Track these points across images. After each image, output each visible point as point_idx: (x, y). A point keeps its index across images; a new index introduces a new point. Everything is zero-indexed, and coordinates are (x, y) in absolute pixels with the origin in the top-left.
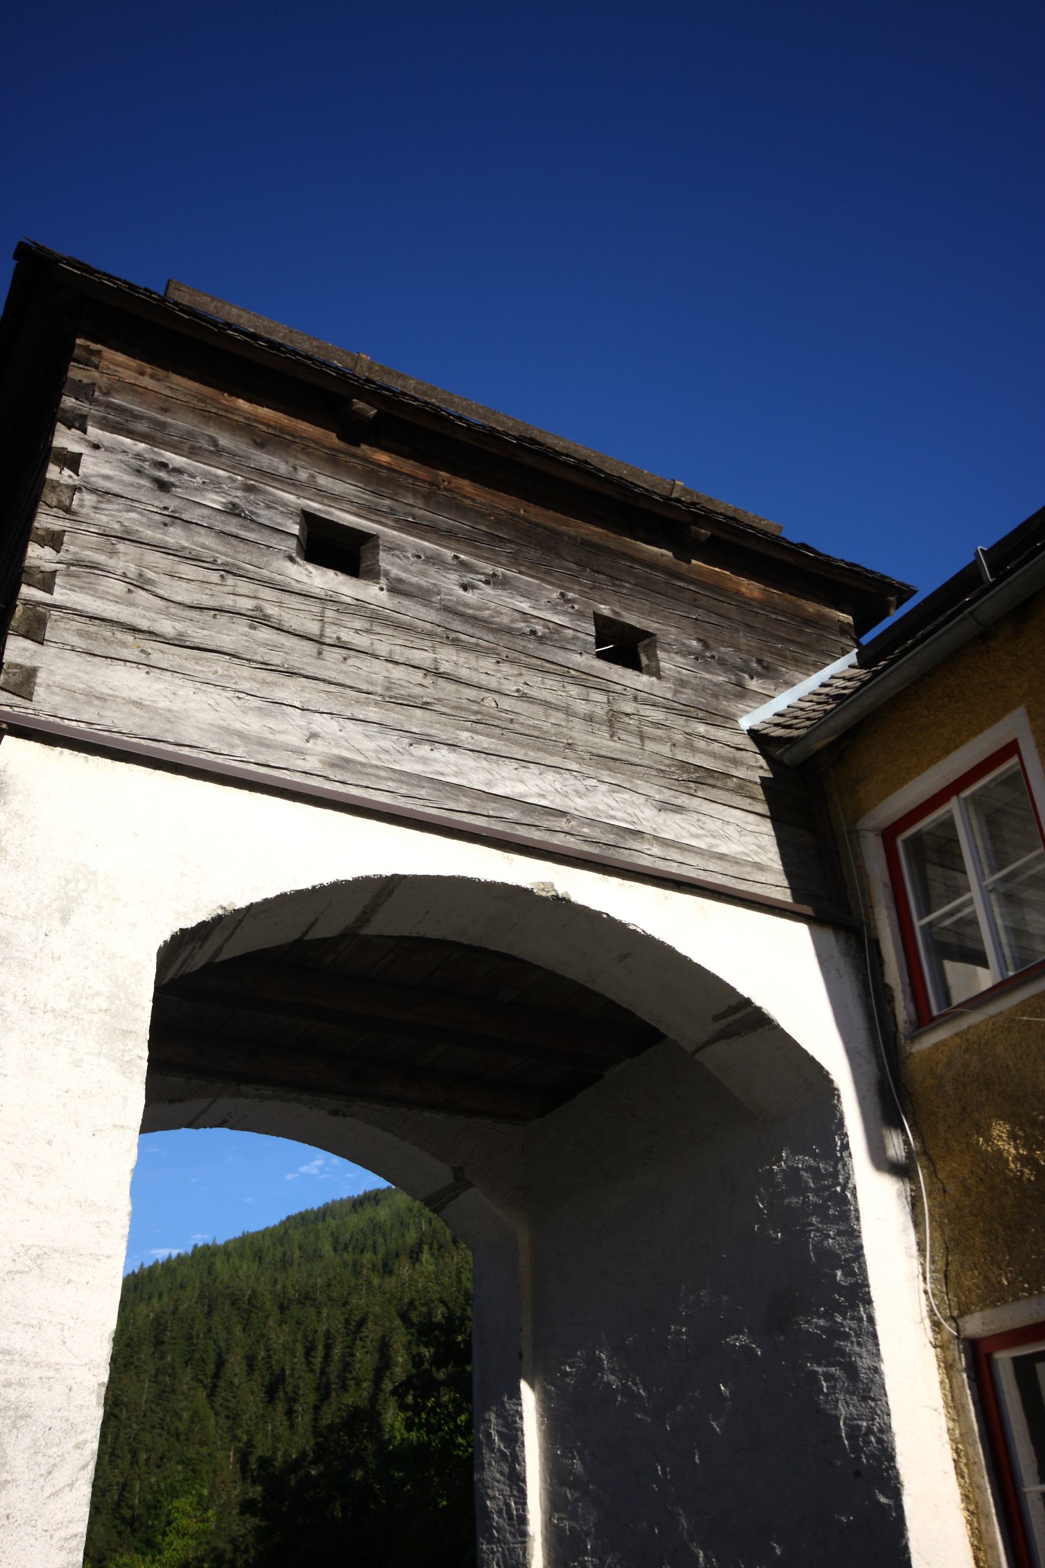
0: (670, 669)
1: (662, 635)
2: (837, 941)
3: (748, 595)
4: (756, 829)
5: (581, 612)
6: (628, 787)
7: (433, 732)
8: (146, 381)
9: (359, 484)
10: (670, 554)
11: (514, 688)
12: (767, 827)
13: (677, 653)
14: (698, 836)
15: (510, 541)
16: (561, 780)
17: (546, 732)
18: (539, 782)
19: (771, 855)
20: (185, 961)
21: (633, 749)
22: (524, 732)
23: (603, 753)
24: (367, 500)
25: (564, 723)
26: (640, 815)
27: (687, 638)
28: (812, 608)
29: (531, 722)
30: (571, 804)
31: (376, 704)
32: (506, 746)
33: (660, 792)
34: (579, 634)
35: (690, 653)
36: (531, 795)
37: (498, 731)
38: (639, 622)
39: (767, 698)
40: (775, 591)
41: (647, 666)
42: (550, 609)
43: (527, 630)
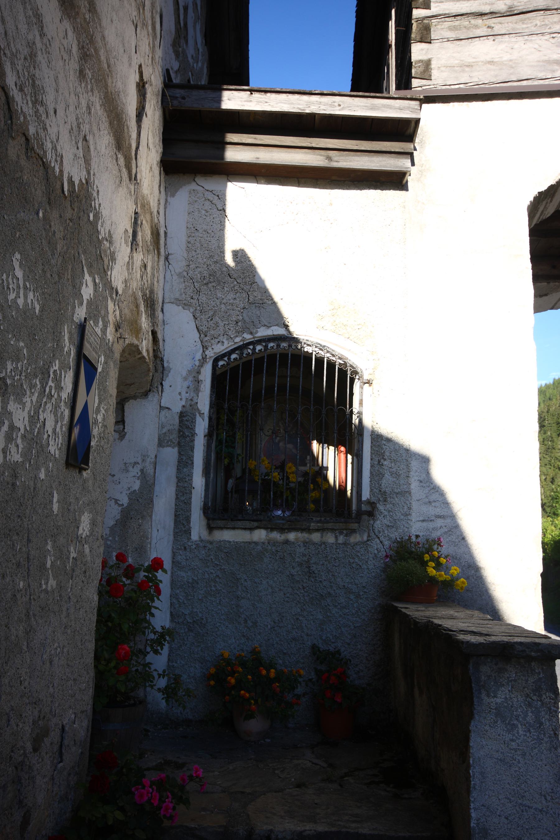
20: (542, 212)
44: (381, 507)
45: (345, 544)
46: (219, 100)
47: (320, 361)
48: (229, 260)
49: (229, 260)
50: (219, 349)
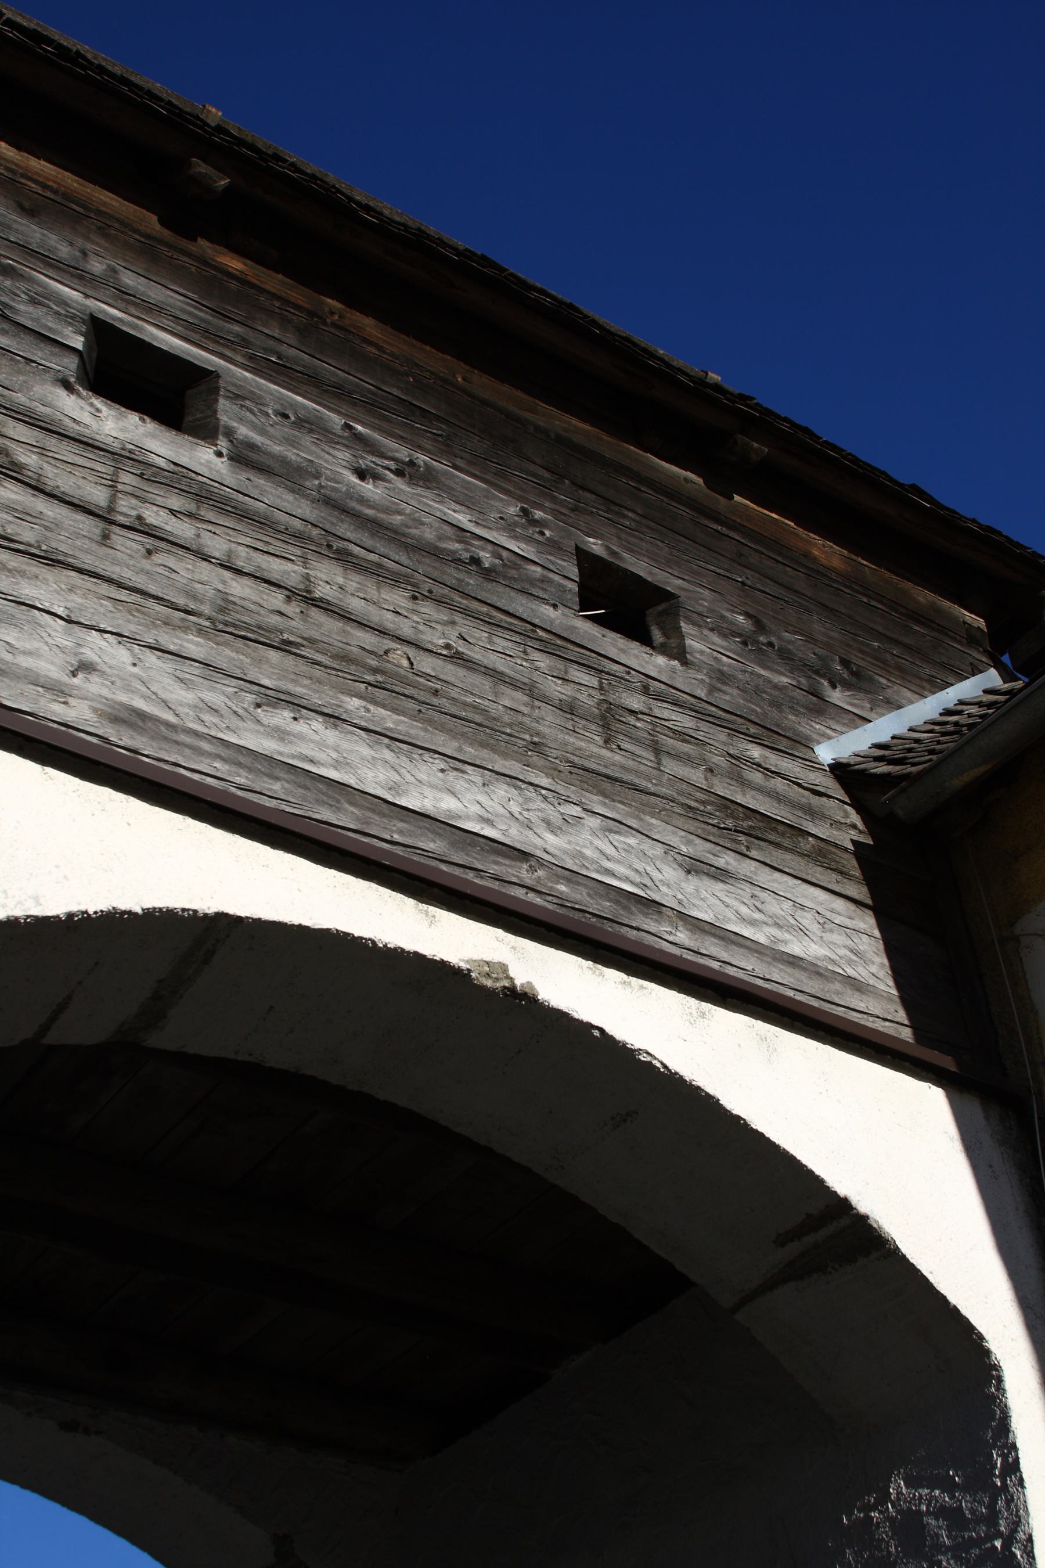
0: (702, 652)
1: (689, 598)
2: (987, 1118)
3: (824, 562)
4: (848, 923)
5: (556, 542)
6: (634, 826)
7: (299, 690)
9: (190, 294)
10: (700, 481)
11: (441, 642)
12: (867, 922)
13: (712, 630)
14: (752, 923)
15: (438, 418)
16: (521, 800)
17: (494, 719)
18: (482, 798)
19: (874, 969)
21: (642, 768)
22: (457, 713)
23: (594, 766)
24: (202, 320)
25: (526, 710)
26: (655, 874)
27: (728, 610)
28: (923, 596)
29: (469, 699)
30: (538, 842)
31: (200, 631)
32: (426, 730)
33: (689, 843)
34: (551, 575)
35: (735, 634)
36: (468, 818)
37: (411, 705)
38: (651, 573)
39: (859, 721)
40: (865, 563)
41: (663, 645)
42: (504, 529)
43: (465, 556)
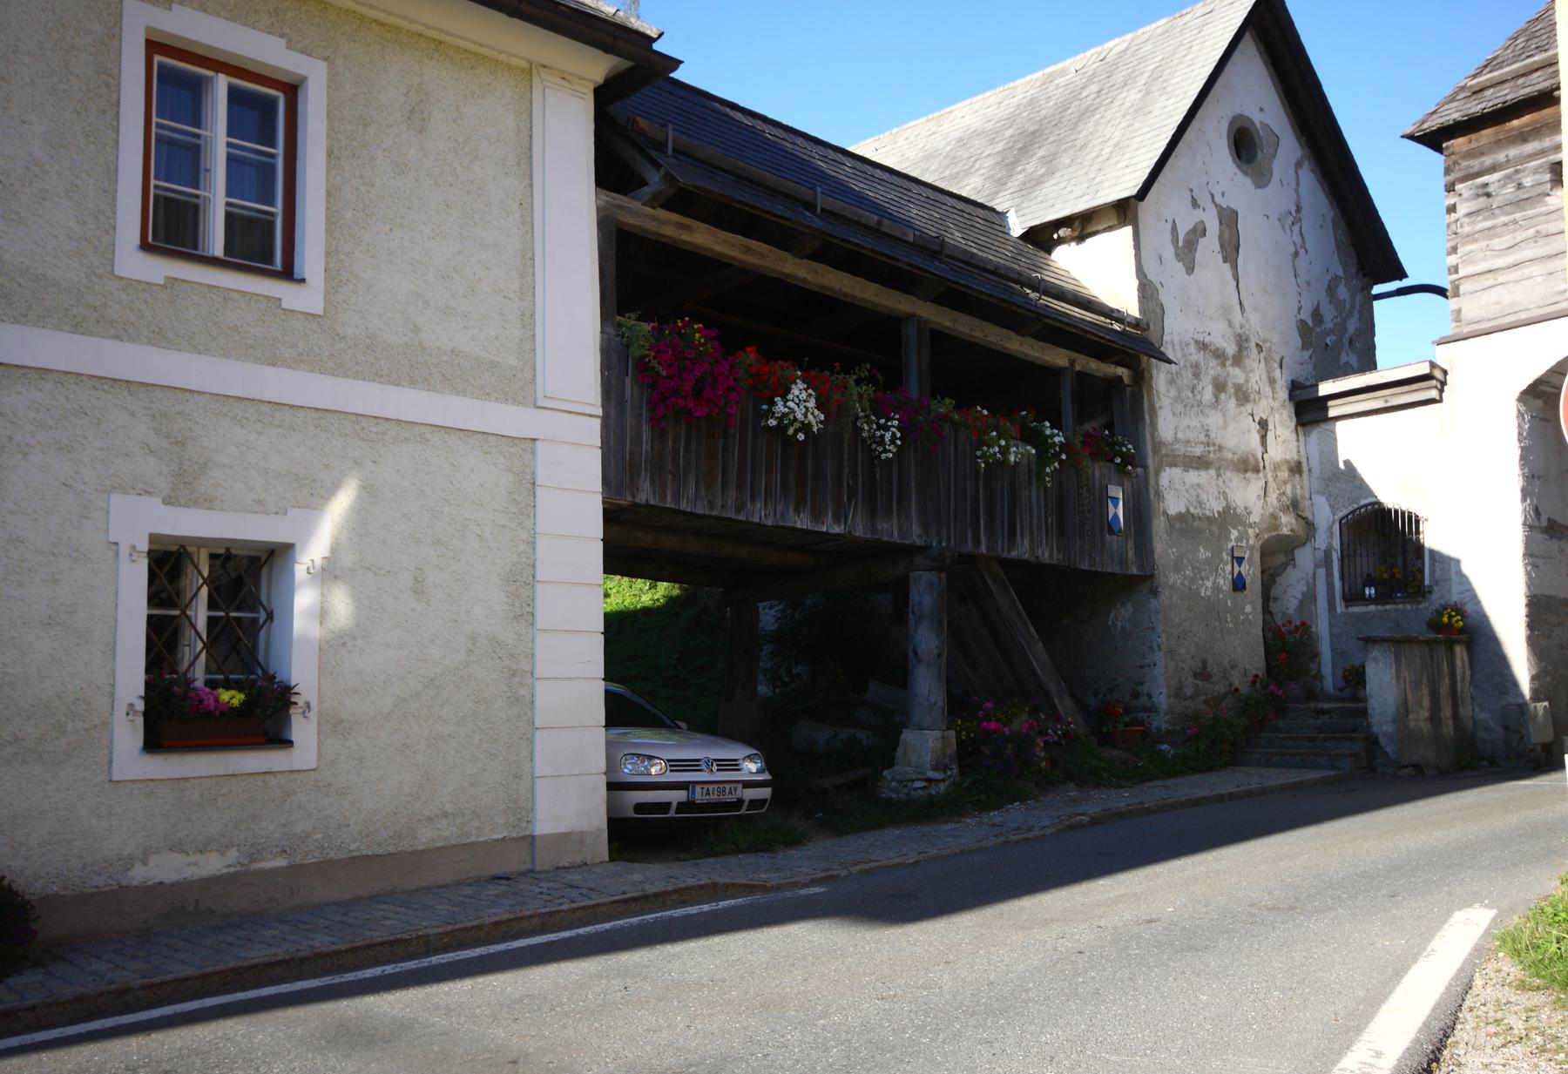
8: (1474, 145)
44: (1435, 588)
45: (1417, 609)
46: (1317, 391)
47: (1396, 511)
48: (1342, 466)
49: (1342, 466)
50: (1341, 514)
